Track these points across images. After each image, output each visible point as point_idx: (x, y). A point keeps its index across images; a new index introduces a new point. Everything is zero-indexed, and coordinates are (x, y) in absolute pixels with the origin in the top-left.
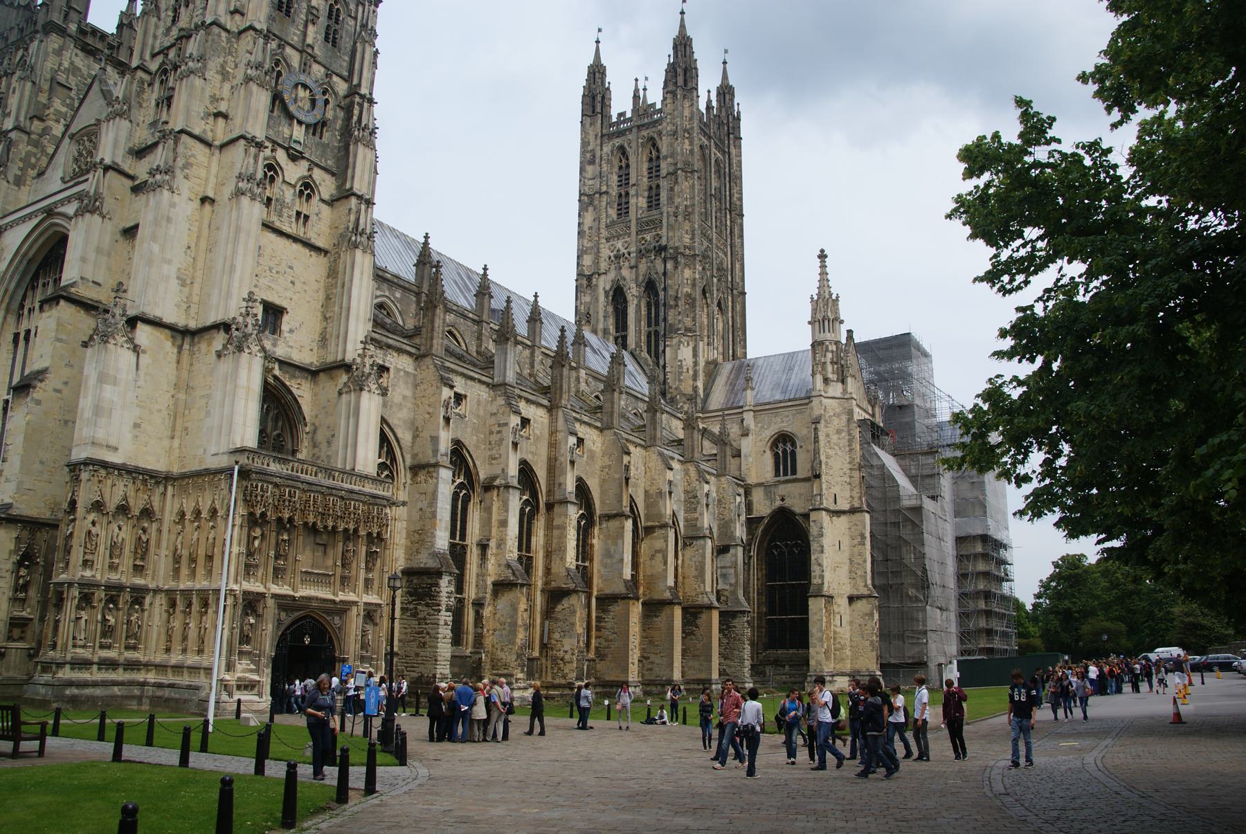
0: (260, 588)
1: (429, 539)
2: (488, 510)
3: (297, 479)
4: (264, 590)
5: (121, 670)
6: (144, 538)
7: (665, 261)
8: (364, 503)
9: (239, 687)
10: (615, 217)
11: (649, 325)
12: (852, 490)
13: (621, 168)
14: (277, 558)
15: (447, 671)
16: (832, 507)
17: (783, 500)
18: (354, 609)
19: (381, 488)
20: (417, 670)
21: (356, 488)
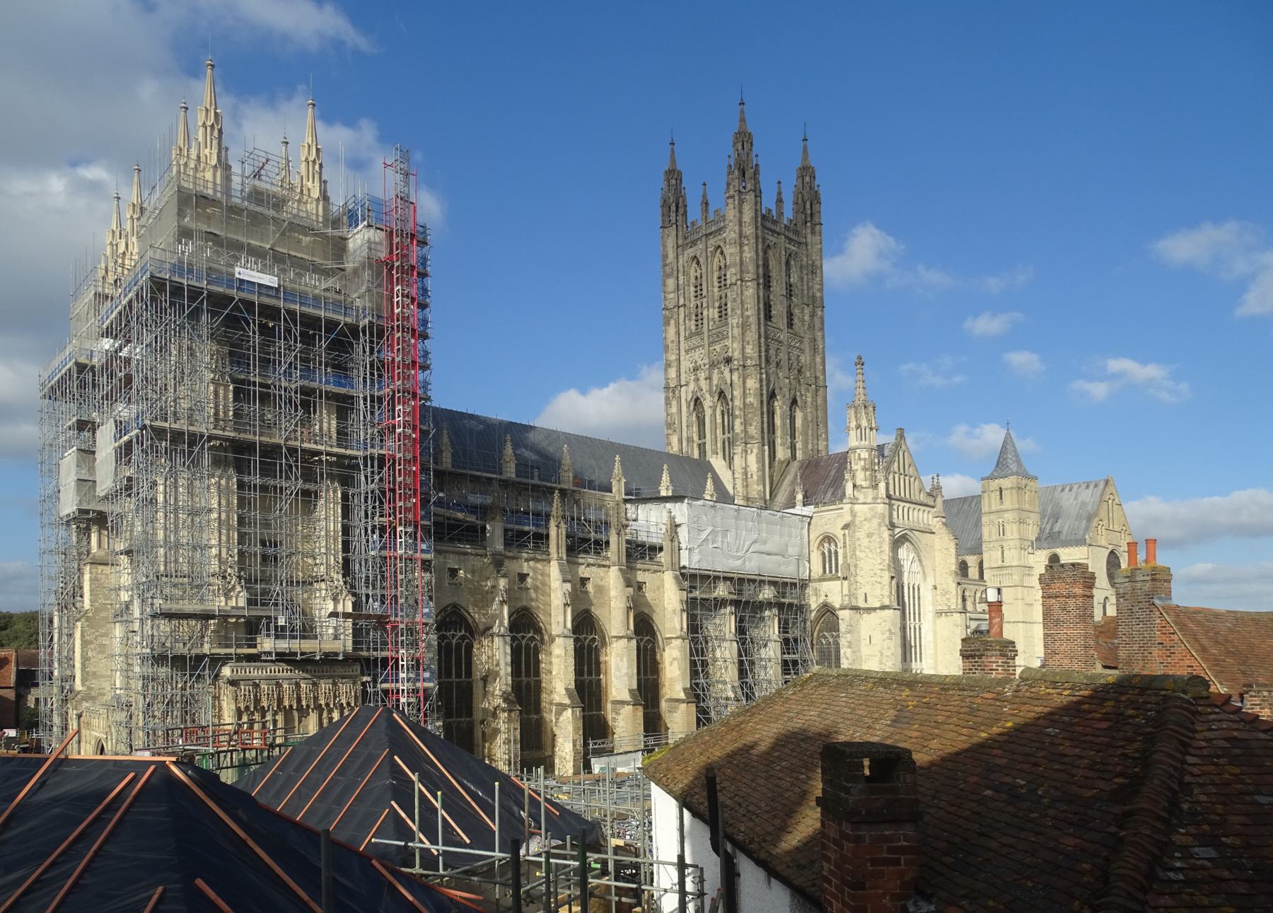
10: (693, 328)
11: (724, 434)
12: (882, 589)
13: (696, 278)
16: (861, 604)
17: (826, 596)
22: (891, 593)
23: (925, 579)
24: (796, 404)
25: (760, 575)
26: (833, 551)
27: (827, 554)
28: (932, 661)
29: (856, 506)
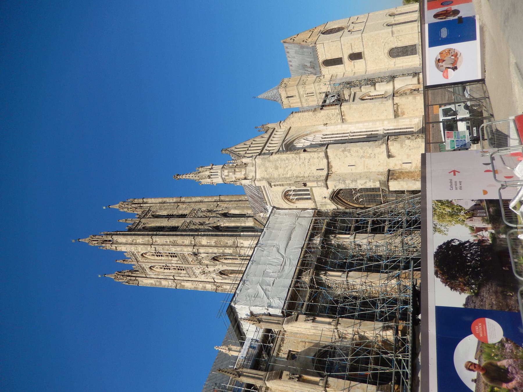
7: (201, 253)
10: (185, 272)
11: (237, 259)
13: (161, 268)
16: (325, 173)
17: (325, 198)
22: (315, 151)
23: (320, 131)
24: (227, 213)
25: (303, 248)
26: (294, 193)
27: (297, 197)
28: (378, 123)
29: (258, 177)
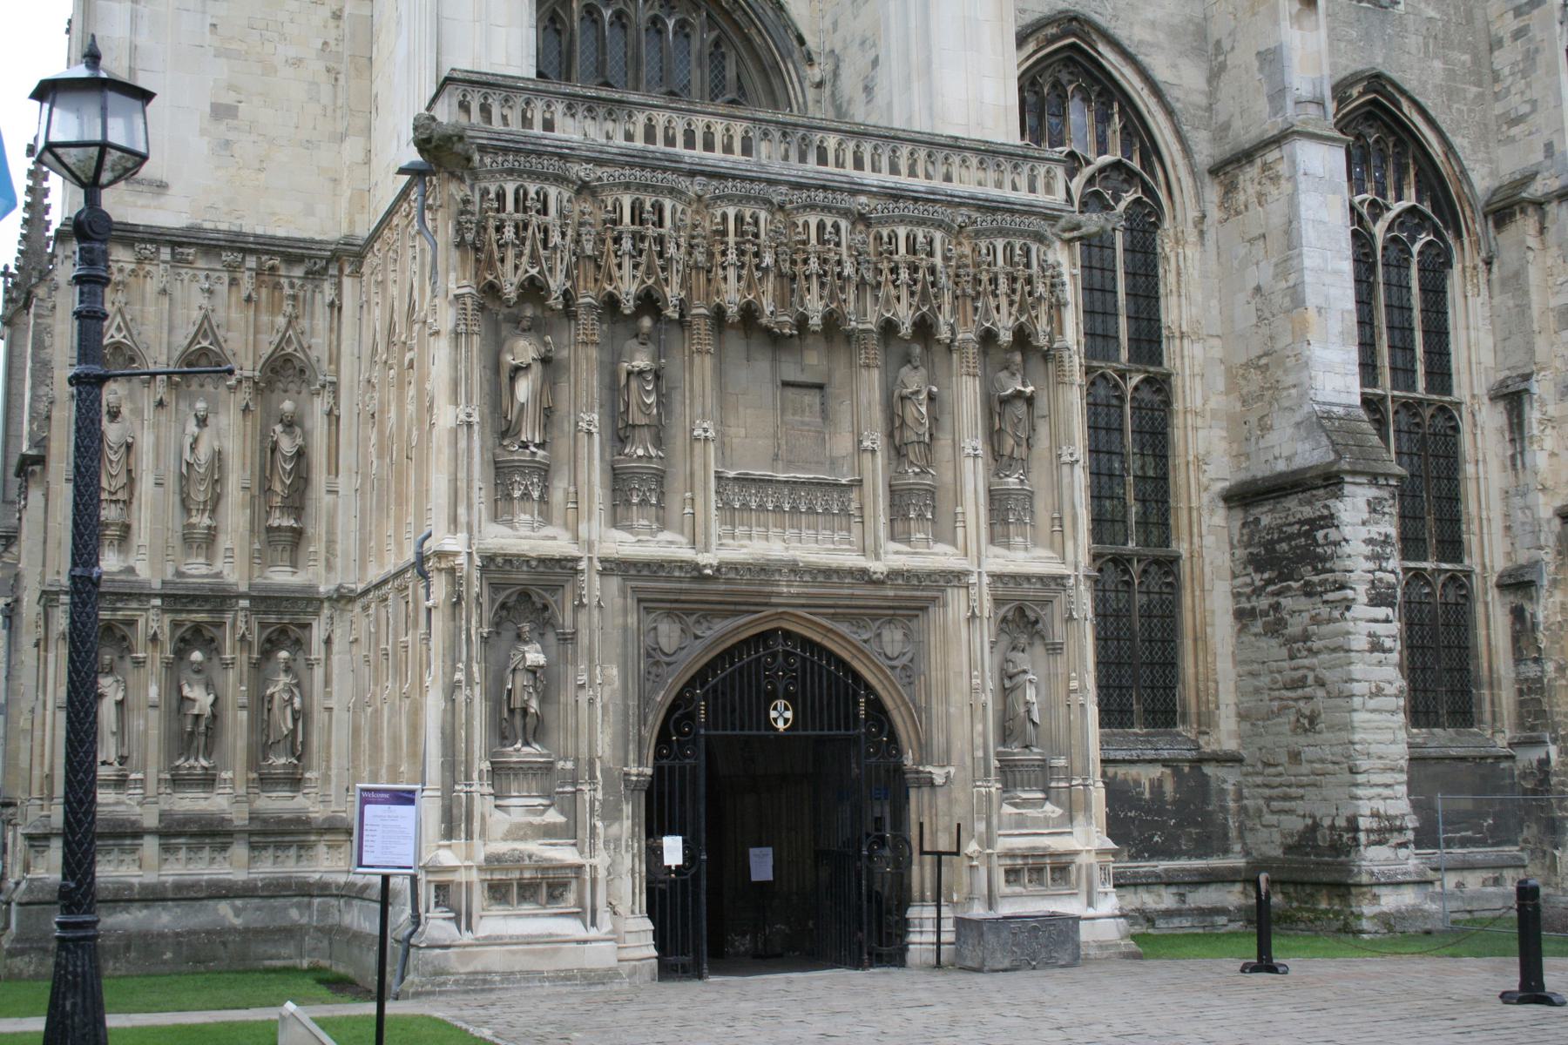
0: (556, 543)
1: (1290, 380)
2: (1516, 282)
3: (672, 165)
4: (572, 550)
5: (240, 851)
6: (287, 446)
8: (956, 232)
9: (498, 892)
14: (620, 434)
15: (1399, 805)
18: (957, 603)
19: (1023, 182)
20: (1299, 806)
21: (919, 184)
